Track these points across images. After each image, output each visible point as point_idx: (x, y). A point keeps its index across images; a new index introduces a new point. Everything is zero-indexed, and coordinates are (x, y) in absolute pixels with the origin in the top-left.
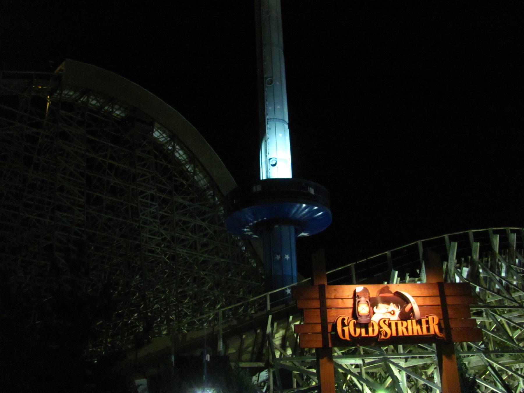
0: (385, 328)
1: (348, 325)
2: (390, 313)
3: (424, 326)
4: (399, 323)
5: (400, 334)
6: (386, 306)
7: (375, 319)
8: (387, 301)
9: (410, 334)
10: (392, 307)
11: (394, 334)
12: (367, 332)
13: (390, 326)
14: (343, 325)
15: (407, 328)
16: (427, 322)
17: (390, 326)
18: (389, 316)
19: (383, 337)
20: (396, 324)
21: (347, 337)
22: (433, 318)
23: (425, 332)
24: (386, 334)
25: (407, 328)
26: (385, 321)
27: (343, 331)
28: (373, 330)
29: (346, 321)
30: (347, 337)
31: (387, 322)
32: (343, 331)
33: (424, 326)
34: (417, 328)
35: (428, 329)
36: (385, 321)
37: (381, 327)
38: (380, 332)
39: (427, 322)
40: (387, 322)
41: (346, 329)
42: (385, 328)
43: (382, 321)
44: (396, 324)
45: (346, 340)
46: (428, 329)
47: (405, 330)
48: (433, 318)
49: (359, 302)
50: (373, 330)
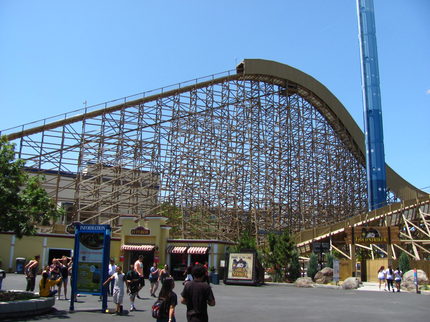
0: (370, 240)
3: (382, 239)
8: (371, 232)
10: (373, 234)
11: (373, 241)
12: (364, 240)
13: (371, 239)
14: (358, 238)
15: (376, 240)
16: (383, 238)
17: (371, 239)
18: (371, 236)
20: (373, 239)
21: (359, 242)
25: (376, 240)
27: (358, 240)
32: (358, 240)
33: (382, 239)
34: (379, 240)
35: (383, 240)
39: (383, 238)
41: (358, 239)
42: (370, 240)
44: (373, 239)
46: (383, 240)
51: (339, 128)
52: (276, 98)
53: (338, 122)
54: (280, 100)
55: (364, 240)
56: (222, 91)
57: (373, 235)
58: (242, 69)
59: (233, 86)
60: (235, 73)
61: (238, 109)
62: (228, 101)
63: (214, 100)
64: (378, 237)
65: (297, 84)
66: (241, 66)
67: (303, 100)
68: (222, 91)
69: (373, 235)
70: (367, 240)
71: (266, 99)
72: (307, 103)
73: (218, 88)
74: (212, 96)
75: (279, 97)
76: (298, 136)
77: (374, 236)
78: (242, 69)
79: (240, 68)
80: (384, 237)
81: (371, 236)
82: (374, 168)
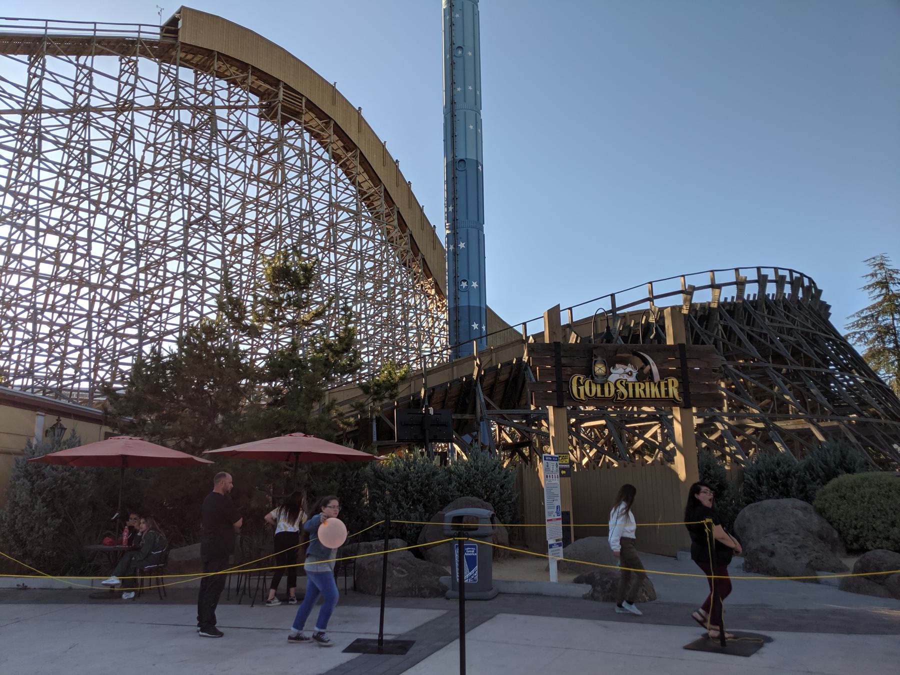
0: (622, 389)
1: (584, 384)
2: (628, 374)
3: (663, 389)
4: (637, 385)
5: (637, 396)
6: (625, 367)
7: (612, 378)
9: (648, 396)
10: (629, 368)
11: (631, 396)
12: (603, 392)
13: (627, 387)
14: (579, 384)
15: (644, 390)
17: (627, 387)
19: (619, 398)
21: (582, 397)
22: (673, 381)
23: (663, 396)
24: (623, 396)
25: (644, 390)
26: (621, 382)
27: (578, 390)
28: (609, 391)
29: (581, 381)
30: (582, 397)
31: (624, 383)
32: (578, 390)
33: (663, 389)
34: (655, 390)
35: (667, 392)
36: (621, 382)
37: (617, 388)
38: (616, 392)
39: (666, 385)
40: (624, 383)
41: (581, 388)
42: (622, 389)
43: (619, 381)
45: (581, 400)
47: (642, 392)
48: (673, 381)
49: (596, 361)
50: (609, 391)
51: (383, 209)
52: (253, 123)
53: (383, 194)
54: (260, 127)
55: (603, 392)
56: (120, 76)
57: (630, 374)
58: (173, 28)
59: (148, 67)
60: (153, 34)
61: (158, 128)
62: (134, 97)
63: (95, 83)
64: (651, 379)
65: (302, 95)
66: (174, 21)
67: (311, 139)
68: (120, 76)
69: (630, 374)
70: (613, 389)
71: (229, 119)
72: (318, 145)
73: (109, 64)
74: (90, 75)
75: (260, 120)
76: (299, 210)
77: (632, 379)
78: (173, 28)
79: (171, 28)
80: (670, 381)
81: (626, 377)
82: (464, 281)
